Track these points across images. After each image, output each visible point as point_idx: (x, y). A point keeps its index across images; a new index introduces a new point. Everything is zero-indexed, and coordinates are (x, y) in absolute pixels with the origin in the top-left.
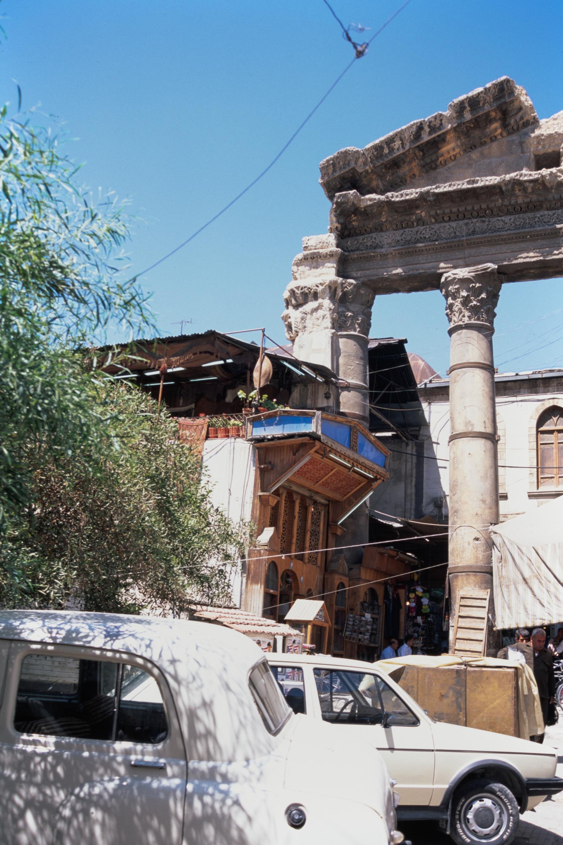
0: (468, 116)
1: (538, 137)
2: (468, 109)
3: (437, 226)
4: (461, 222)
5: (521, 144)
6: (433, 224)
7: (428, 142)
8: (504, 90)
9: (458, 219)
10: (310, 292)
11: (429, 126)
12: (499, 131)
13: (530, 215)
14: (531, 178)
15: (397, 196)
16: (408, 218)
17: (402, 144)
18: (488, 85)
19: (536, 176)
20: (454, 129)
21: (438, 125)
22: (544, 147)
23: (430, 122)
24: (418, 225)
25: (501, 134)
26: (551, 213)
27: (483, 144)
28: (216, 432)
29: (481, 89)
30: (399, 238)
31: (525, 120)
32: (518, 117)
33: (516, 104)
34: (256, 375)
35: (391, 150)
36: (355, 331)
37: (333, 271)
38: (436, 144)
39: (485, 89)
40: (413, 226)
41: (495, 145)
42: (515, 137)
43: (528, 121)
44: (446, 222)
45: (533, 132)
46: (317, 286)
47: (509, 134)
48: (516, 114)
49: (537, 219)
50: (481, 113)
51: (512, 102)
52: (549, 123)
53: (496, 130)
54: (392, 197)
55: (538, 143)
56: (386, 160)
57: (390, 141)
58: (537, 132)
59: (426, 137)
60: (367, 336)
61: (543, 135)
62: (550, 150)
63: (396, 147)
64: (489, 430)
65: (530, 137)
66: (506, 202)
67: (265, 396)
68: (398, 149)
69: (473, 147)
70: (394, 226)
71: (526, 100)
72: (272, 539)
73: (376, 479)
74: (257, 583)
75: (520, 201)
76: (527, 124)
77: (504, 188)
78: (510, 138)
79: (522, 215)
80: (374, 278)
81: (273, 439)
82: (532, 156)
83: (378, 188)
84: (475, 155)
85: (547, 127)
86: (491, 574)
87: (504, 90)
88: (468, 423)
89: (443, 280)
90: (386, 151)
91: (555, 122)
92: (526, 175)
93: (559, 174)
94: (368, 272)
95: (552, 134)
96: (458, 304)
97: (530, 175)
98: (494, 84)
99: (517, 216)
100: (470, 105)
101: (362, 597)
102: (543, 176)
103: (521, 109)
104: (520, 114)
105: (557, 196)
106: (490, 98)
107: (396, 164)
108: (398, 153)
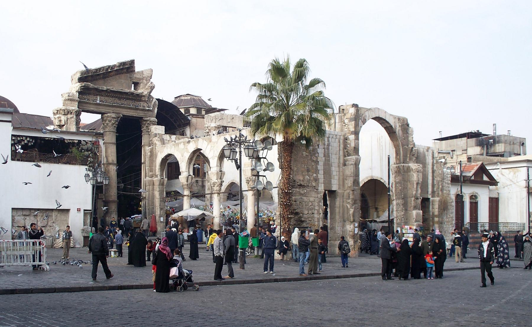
27: (120, 74)
59: (109, 70)
89: (106, 115)
96: (110, 124)
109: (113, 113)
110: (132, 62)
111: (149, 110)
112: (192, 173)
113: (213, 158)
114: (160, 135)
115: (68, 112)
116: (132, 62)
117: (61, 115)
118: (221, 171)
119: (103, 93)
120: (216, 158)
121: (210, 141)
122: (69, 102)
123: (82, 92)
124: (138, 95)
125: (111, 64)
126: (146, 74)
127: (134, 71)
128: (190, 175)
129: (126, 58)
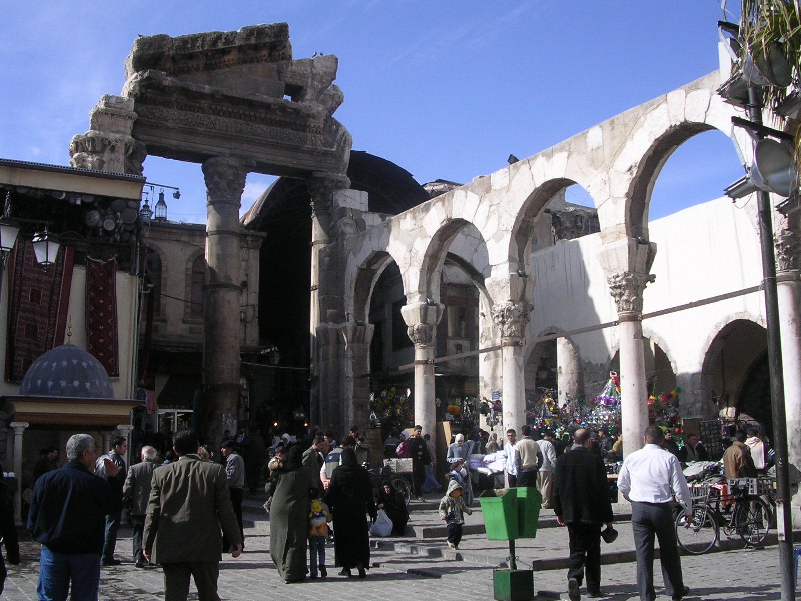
0: (253, 41)
3: (213, 117)
4: (232, 120)
6: (210, 114)
7: (219, 49)
9: (230, 116)
10: (109, 144)
11: (225, 38)
13: (279, 129)
16: (193, 104)
17: (202, 44)
20: (240, 47)
21: (231, 39)
23: (228, 35)
24: (198, 111)
26: (295, 132)
27: (252, 61)
35: (193, 45)
37: (129, 131)
38: (224, 52)
40: (194, 111)
41: (260, 66)
42: (274, 65)
44: (220, 116)
46: (116, 141)
47: (271, 61)
49: (285, 135)
53: (265, 56)
56: (187, 52)
57: (194, 39)
59: (220, 45)
63: (198, 44)
66: (268, 116)
68: (198, 47)
69: (245, 62)
70: (180, 107)
75: (278, 118)
77: (272, 106)
79: (275, 128)
80: (156, 144)
83: (169, 69)
84: (245, 68)
88: (228, 278)
89: (212, 160)
90: (189, 46)
94: (153, 138)
96: (223, 184)
99: (272, 128)
103: (285, 46)
104: (283, 51)
107: (191, 57)
108: (197, 50)
109: (232, 155)
110: (282, 30)
111: (326, 154)
112: (437, 299)
113: (497, 237)
114: (358, 212)
115: (104, 146)
116: (282, 30)
117: (84, 154)
118: (523, 276)
119: (205, 103)
120: (508, 237)
121: (488, 189)
122: (107, 120)
123: (145, 94)
124: (297, 111)
125: (226, 29)
126: (320, 68)
127: (290, 57)
128: (432, 304)
129: (264, 18)
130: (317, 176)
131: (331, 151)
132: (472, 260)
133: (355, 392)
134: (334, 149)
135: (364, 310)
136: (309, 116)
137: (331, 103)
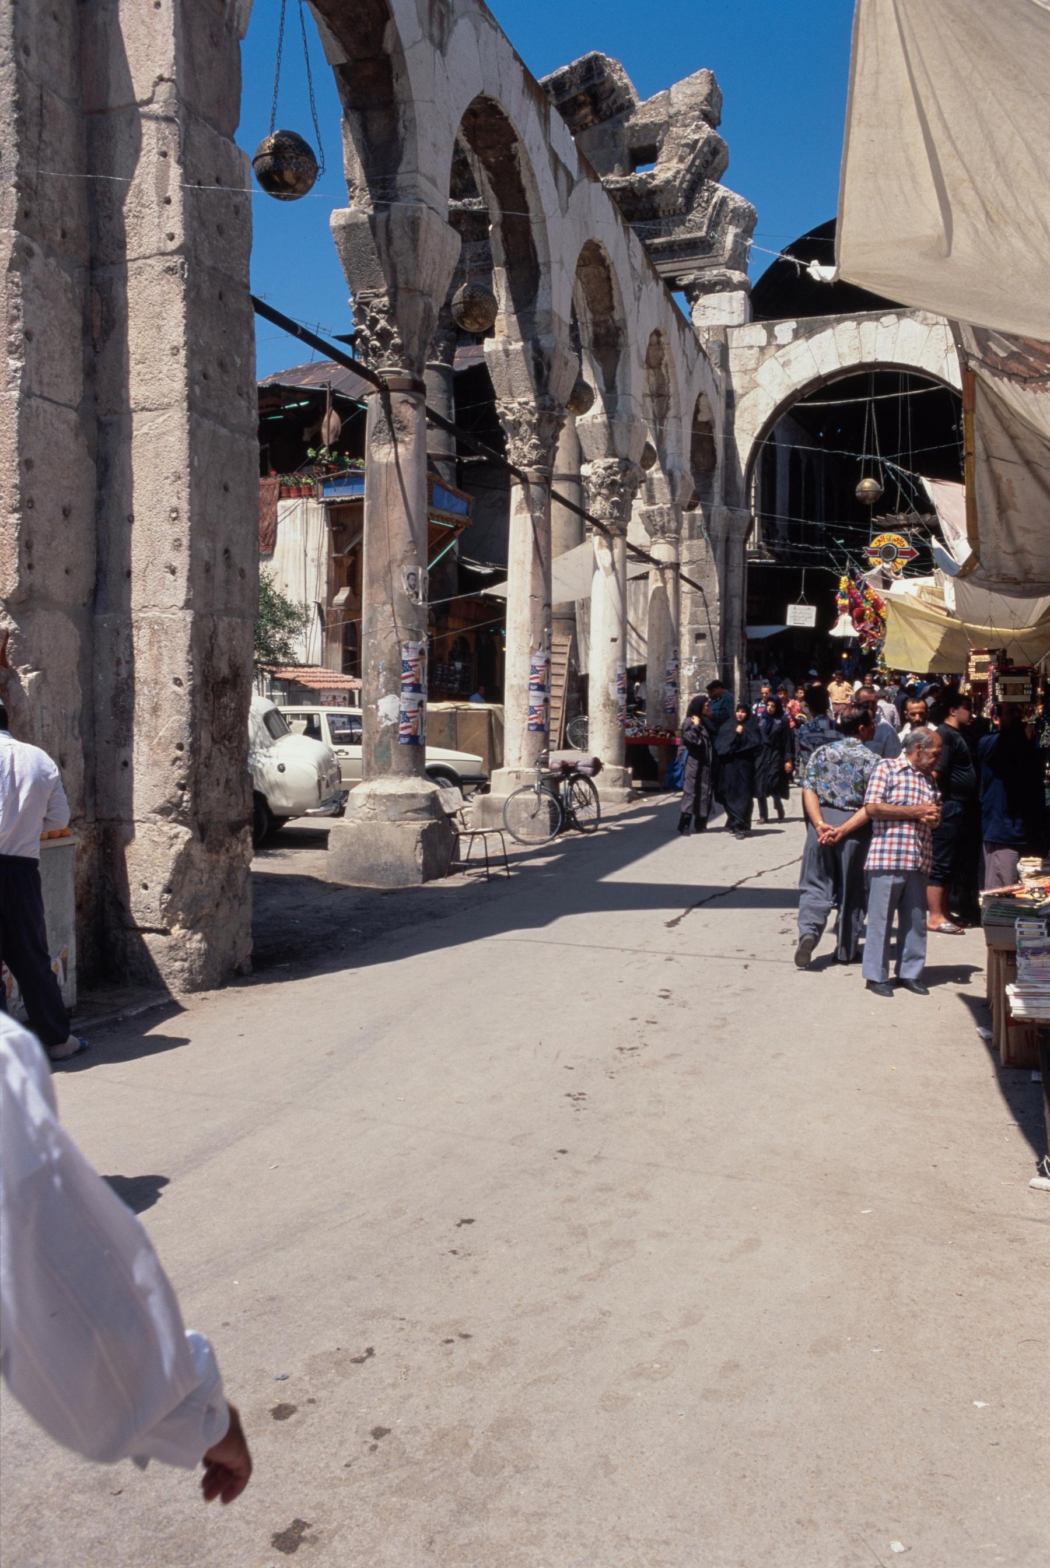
1: (632, 128)
2: (553, 92)
5: (614, 134)
8: (592, 69)
12: (590, 118)
14: (618, 186)
15: (475, 204)
18: (574, 64)
19: (624, 184)
22: (638, 140)
25: (592, 121)
28: (288, 491)
29: (566, 68)
30: (480, 251)
31: (619, 103)
32: (610, 101)
33: (607, 85)
34: (324, 431)
36: (437, 359)
39: (571, 68)
42: (607, 125)
43: (622, 105)
45: (628, 120)
47: (602, 120)
48: (609, 97)
50: (567, 98)
51: (603, 83)
52: (647, 108)
53: (586, 116)
54: (470, 204)
55: (633, 135)
58: (633, 120)
60: (452, 364)
61: (637, 125)
62: (645, 144)
64: (574, 472)
65: (623, 126)
67: (335, 453)
71: (621, 77)
72: (347, 599)
73: (457, 528)
74: (335, 641)
76: (621, 108)
78: (602, 127)
81: (342, 502)
82: (626, 151)
85: (645, 113)
86: (574, 620)
87: (592, 69)
91: (653, 106)
92: (612, 182)
93: (650, 180)
95: (647, 124)
97: (618, 182)
98: (580, 62)
100: (554, 88)
101: (450, 645)
102: (631, 184)
103: (613, 90)
104: (613, 97)
105: (647, 206)
106: (576, 79)
130: (683, 283)
131: (700, 238)
132: (941, 368)
133: (693, 615)
134: (702, 234)
135: (711, 485)
136: (653, 192)
137: (692, 156)
